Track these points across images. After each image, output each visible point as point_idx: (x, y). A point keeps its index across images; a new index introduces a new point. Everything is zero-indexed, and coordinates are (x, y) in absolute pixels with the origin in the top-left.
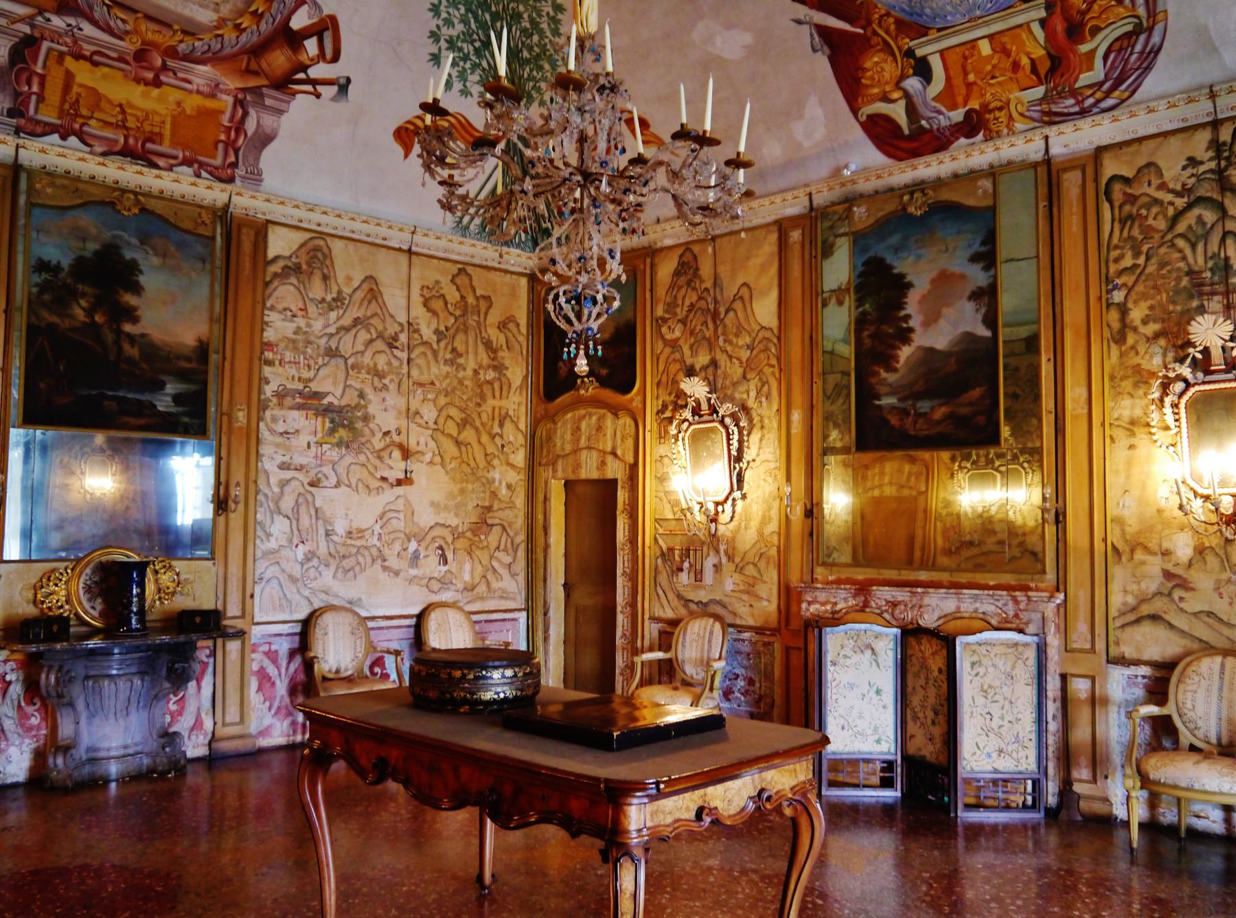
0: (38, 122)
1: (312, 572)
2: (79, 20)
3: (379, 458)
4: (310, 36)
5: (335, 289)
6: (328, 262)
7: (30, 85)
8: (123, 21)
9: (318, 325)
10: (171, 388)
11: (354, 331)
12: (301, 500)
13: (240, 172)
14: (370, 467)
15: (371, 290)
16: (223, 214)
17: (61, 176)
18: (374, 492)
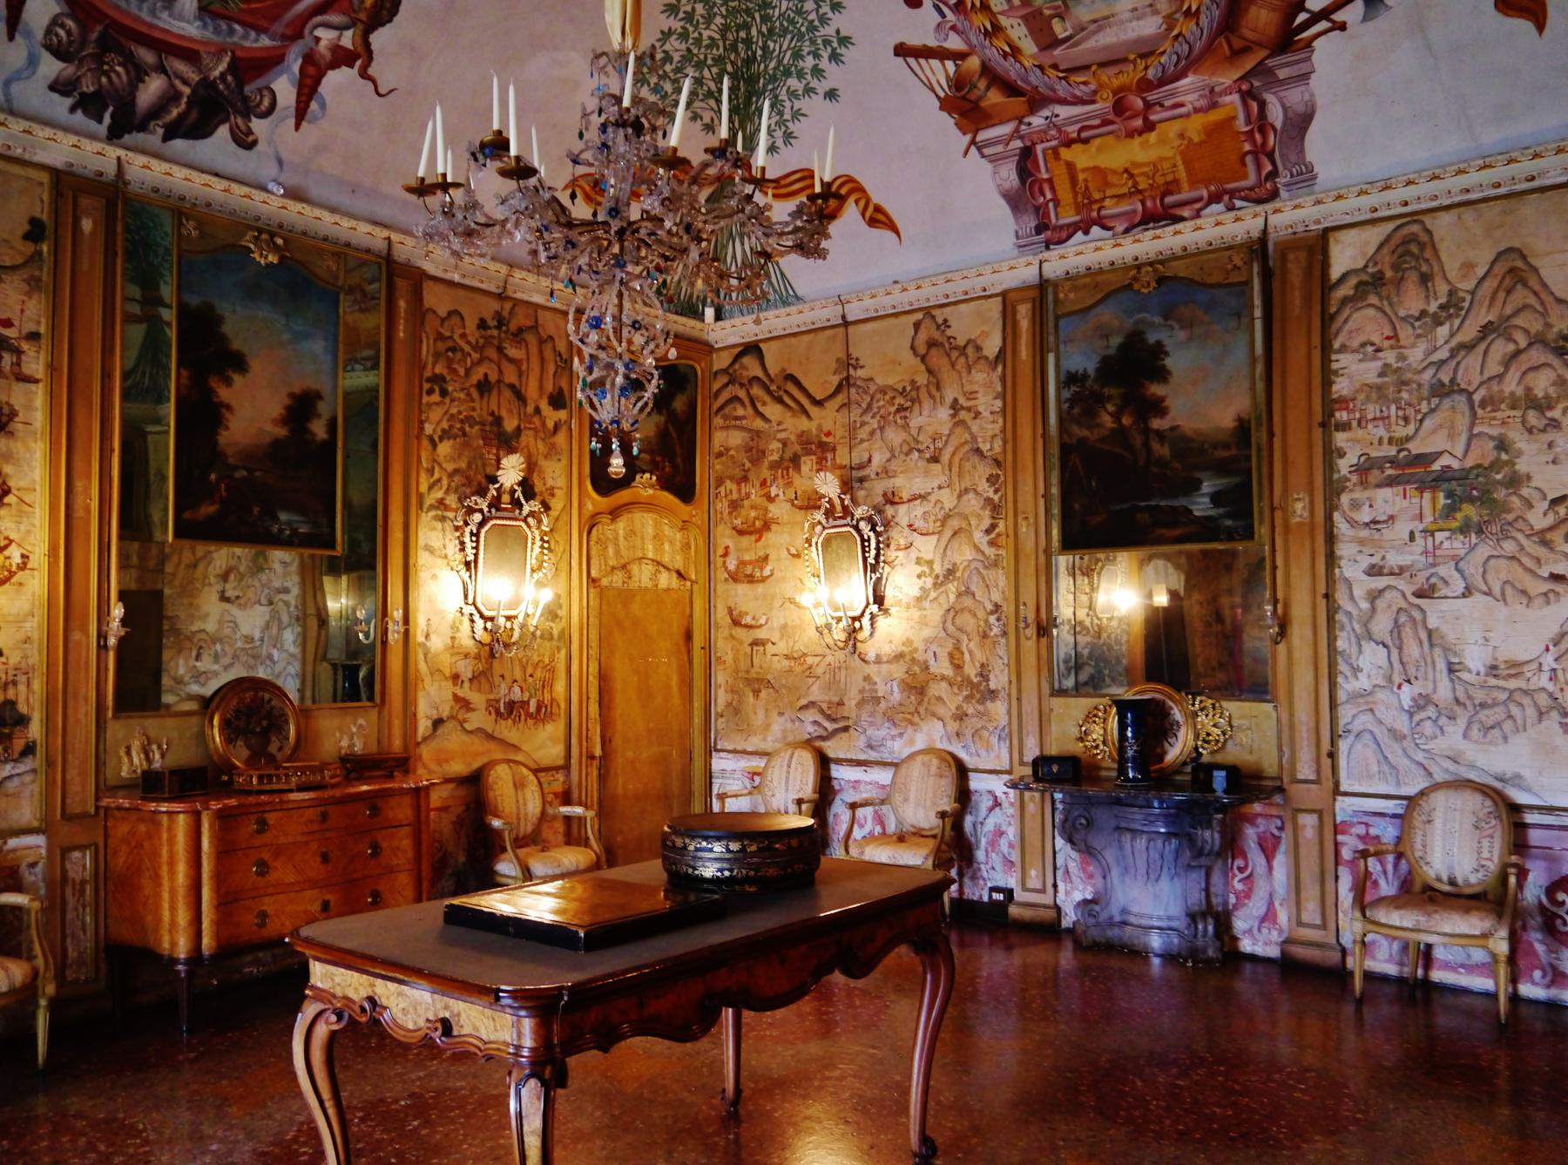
0: (1061, 227)
1: (1428, 728)
3: (1545, 543)
5: (1442, 289)
6: (1428, 254)
8: (1085, 83)
9: (1416, 355)
10: (1207, 487)
11: (1483, 346)
12: (1403, 619)
14: (1525, 560)
15: (1512, 270)
17: (1086, 276)
18: (1540, 600)
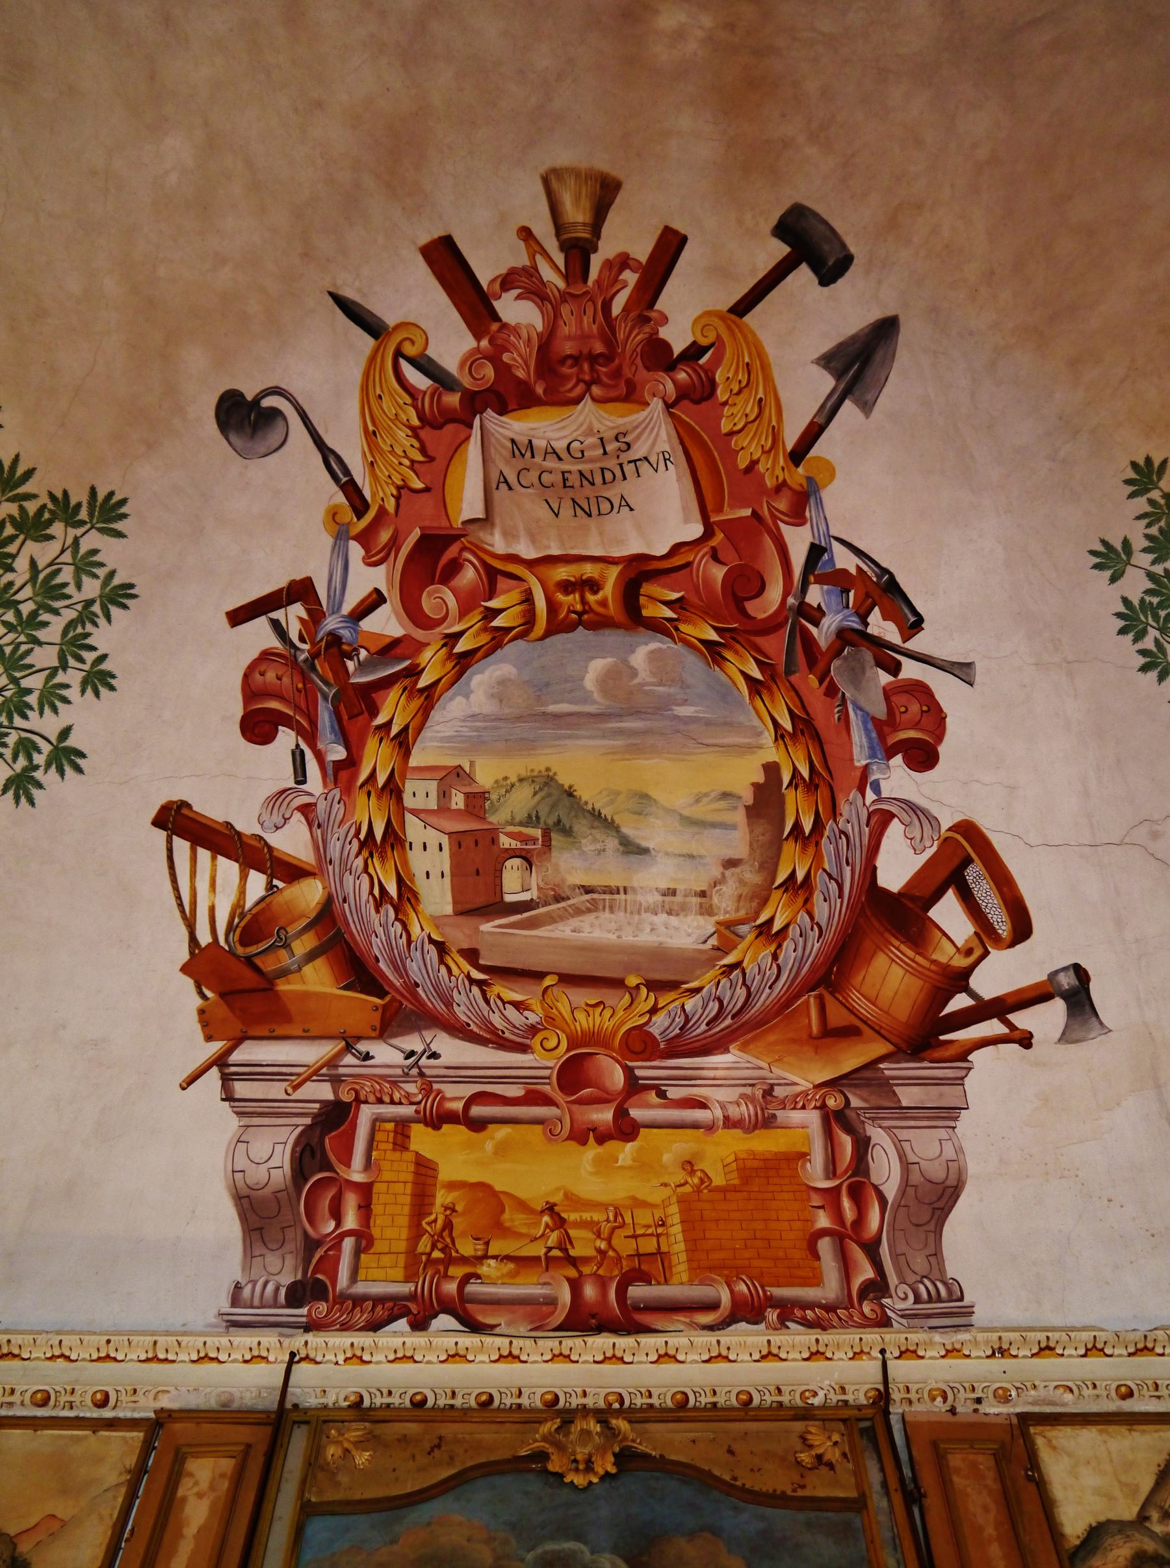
0: (358, 1301)
2: (428, 1035)
4: (936, 896)
7: (337, 1214)
8: (518, 1006)
13: (898, 1302)
16: (868, 1420)
